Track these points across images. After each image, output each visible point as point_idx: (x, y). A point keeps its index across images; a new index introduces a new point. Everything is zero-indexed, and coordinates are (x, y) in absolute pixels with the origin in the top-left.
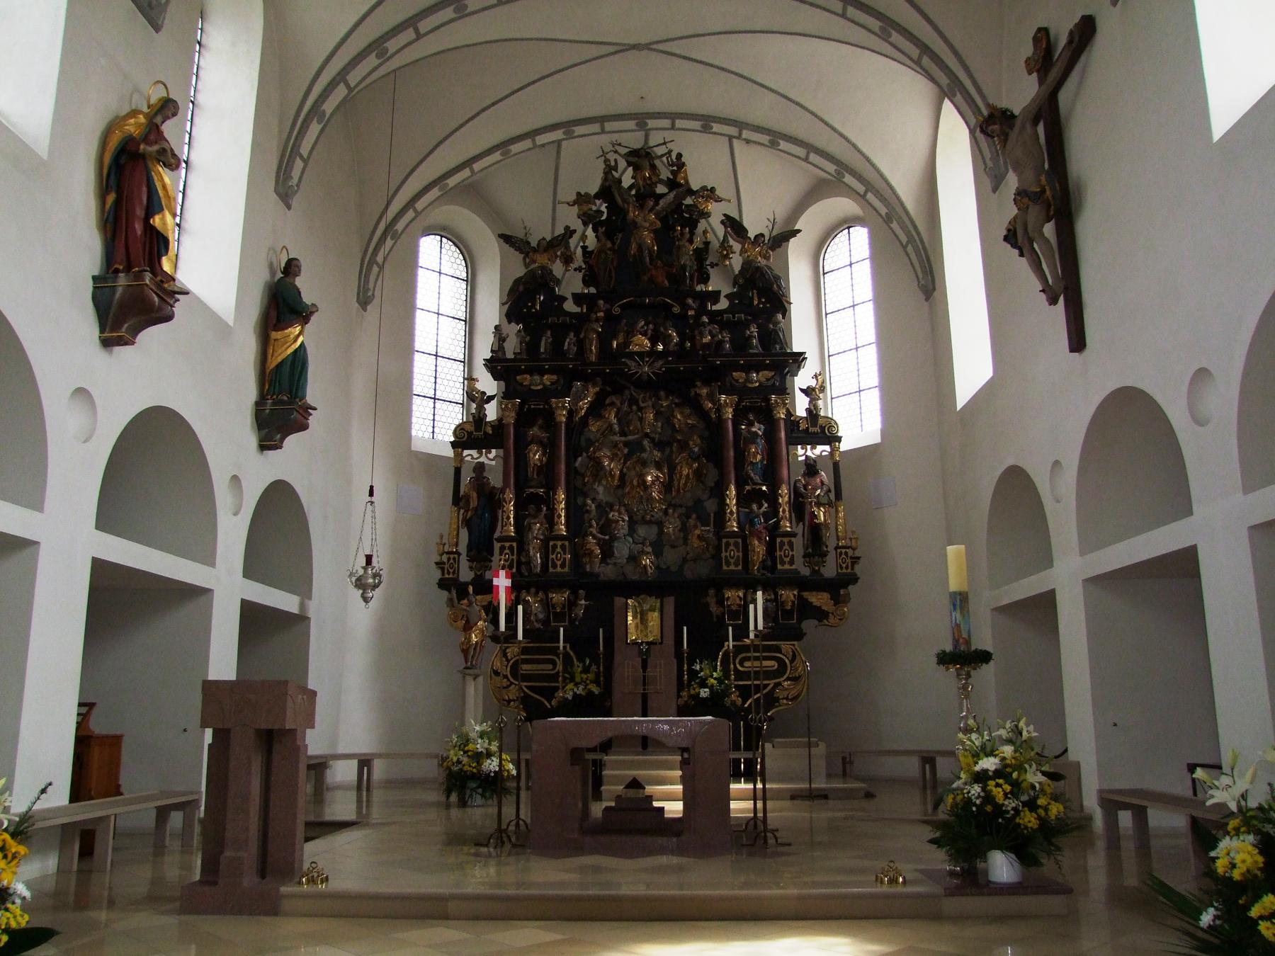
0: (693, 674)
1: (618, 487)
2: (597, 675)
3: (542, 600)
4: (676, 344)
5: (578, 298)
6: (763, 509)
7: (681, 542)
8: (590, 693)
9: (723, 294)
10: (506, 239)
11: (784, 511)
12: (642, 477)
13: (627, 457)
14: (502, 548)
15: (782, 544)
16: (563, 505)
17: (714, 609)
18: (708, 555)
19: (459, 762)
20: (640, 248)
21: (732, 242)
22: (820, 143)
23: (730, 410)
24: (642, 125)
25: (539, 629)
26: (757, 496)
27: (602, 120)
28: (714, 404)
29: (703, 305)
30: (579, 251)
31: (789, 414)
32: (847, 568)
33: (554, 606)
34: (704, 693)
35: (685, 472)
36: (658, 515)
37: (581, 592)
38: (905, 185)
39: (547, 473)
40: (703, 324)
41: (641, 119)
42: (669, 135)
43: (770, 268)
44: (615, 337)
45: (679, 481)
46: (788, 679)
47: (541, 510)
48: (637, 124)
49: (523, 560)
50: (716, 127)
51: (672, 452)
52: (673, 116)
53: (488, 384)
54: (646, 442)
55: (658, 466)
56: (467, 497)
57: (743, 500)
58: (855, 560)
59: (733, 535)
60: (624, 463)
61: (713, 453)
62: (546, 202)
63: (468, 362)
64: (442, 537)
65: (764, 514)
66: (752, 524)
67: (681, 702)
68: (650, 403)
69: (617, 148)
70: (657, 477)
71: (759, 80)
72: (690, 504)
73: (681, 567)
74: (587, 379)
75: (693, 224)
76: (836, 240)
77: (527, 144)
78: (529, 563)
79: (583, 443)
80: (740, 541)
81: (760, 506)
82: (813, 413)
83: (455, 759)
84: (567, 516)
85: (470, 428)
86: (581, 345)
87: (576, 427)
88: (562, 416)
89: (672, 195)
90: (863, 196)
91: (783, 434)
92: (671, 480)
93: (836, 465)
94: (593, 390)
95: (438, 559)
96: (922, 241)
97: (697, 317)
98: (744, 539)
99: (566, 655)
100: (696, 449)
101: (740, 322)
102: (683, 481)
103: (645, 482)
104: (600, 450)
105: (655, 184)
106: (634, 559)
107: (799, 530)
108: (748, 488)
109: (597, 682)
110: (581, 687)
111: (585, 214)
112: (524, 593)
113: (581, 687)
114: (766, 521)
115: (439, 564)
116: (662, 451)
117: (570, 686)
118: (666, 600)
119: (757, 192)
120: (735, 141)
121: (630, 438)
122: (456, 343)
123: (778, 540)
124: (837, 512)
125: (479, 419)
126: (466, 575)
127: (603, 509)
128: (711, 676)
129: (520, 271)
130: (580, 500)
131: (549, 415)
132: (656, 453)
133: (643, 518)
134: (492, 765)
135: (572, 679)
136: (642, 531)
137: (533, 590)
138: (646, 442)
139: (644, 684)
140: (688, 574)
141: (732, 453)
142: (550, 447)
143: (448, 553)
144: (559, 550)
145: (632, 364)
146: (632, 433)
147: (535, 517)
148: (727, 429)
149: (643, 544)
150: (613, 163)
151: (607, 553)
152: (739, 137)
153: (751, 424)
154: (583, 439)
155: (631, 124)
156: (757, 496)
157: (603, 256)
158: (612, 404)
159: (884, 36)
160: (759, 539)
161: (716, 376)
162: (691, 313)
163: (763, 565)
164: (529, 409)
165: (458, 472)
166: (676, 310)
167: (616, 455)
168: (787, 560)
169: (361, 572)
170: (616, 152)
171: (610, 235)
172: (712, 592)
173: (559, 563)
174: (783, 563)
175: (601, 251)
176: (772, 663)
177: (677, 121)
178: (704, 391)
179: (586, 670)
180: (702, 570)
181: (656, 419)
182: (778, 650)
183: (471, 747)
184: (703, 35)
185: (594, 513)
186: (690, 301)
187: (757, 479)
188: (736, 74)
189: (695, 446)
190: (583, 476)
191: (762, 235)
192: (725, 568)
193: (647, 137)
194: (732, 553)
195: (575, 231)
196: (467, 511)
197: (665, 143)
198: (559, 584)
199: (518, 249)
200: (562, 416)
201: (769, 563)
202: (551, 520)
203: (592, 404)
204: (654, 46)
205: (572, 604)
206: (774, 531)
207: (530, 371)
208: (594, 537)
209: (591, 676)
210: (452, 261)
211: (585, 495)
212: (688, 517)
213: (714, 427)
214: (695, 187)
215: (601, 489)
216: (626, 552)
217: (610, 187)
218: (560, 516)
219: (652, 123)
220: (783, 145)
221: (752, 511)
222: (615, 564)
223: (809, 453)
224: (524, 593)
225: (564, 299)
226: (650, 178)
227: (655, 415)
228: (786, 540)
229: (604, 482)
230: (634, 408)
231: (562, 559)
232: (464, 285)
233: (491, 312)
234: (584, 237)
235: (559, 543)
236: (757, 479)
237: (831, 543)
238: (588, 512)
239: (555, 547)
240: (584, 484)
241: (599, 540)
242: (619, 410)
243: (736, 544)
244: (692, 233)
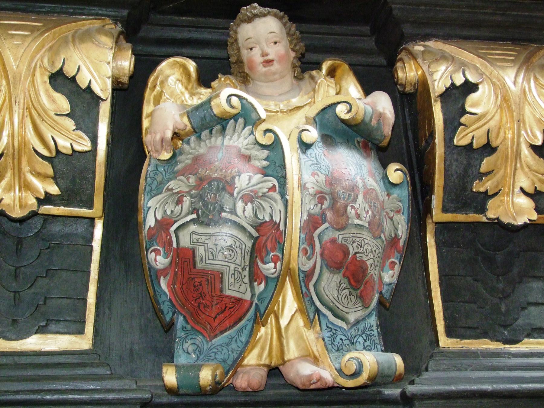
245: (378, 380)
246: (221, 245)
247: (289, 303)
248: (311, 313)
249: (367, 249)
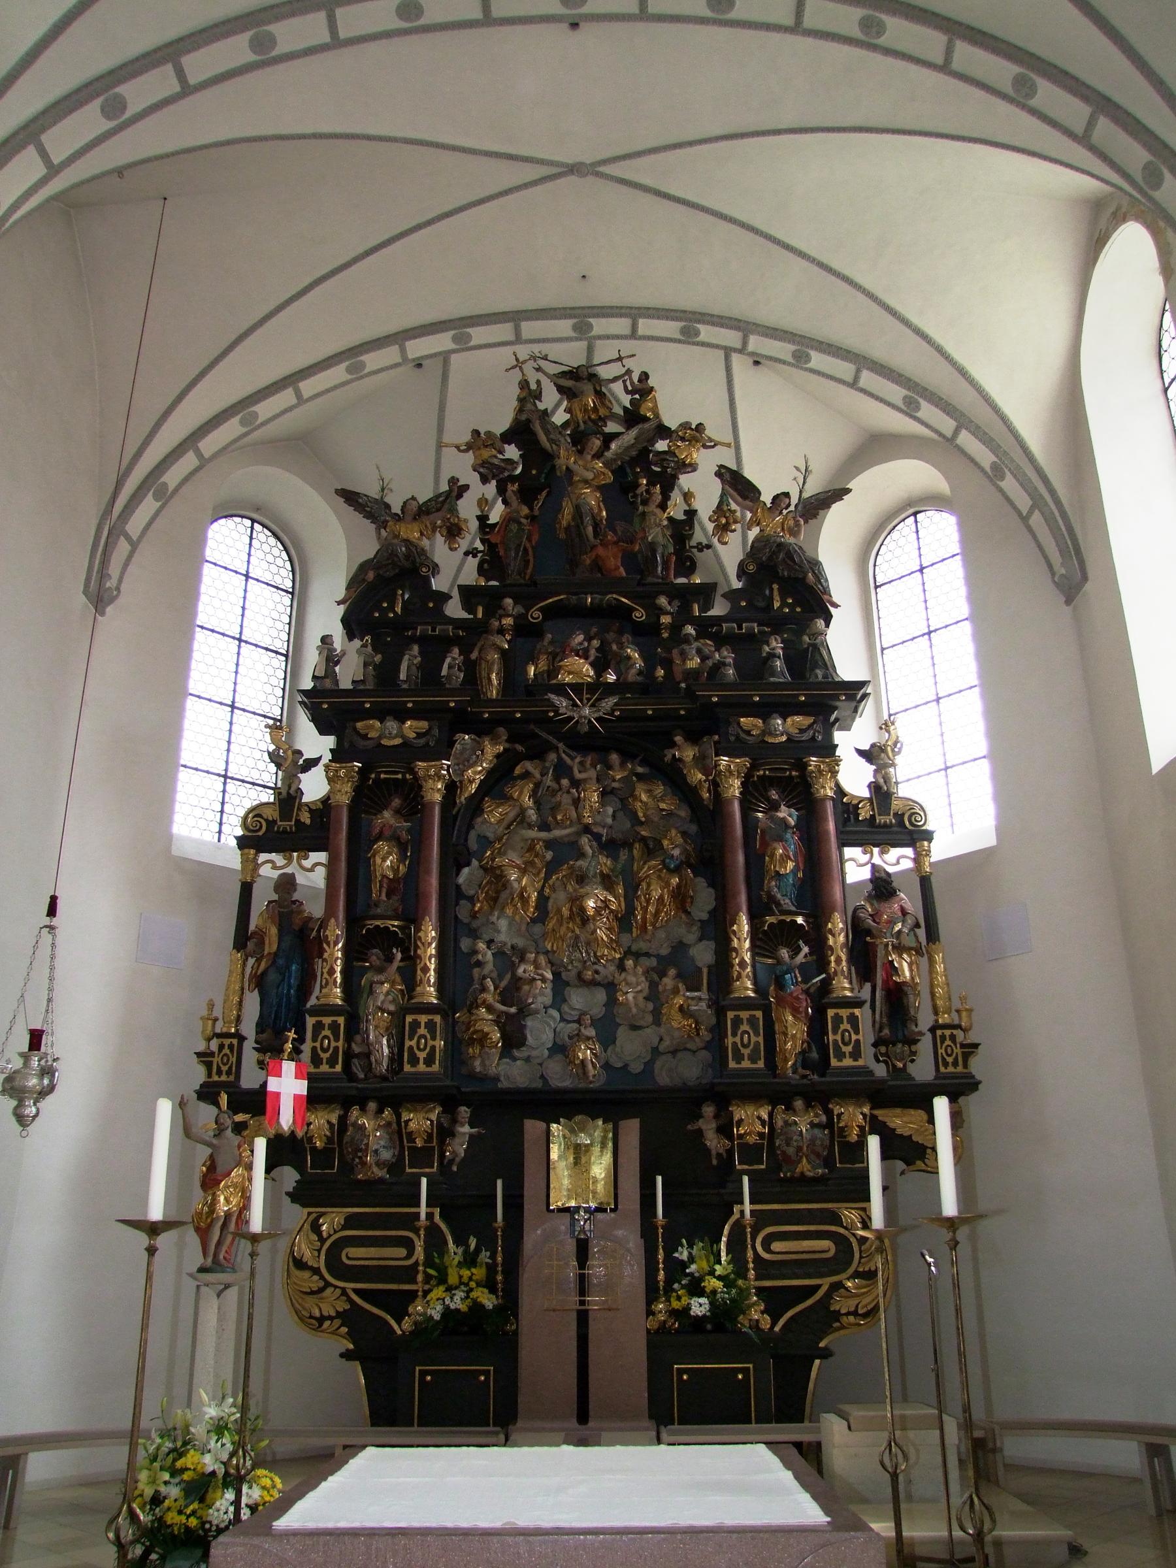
0: (677, 1268)
1: (534, 921)
2: (491, 1269)
3: (389, 1124)
4: (640, 673)
5: (469, 595)
6: (800, 958)
7: (650, 1018)
8: (476, 1307)
9: (721, 591)
10: (350, 497)
11: (838, 961)
12: (577, 903)
13: (552, 868)
14: (318, 1027)
15: (838, 1019)
16: (432, 950)
17: (714, 1142)
18: (698, 1042)
19: (157, 1500)
20: (577, 508)
21: (734, 506)
22: (878, 352)
23: (737, 783)
24: (582, 329)
25: (381, 1180)
26: (788, 934)
27: (516, 317)
28: (706, 772)
29: (685, 608)
30: (474, 525)
31: (840, 792)
32: (955, 1064)
33: (411, 1136)
34: (699, 1307)
35: (656, 893)
36: (608, 971)
37: (463, 1109)
38: (1027, 411)
39: (406, 891)
40: (686, 640)
41: (582, 318)
42: (627, 347)
43: (800, 548)
44: (533, 660)
45: (645, 910)
46: (856, 1275)
47: (390, 959)
48: (575, 328)
49: (356, 1049)
50: (706, 332)
51: (632, 858)
52: (635, 313)
54: (585, 841)
55: (607, 882)
56: (260, 935)
57: (763, 942)
58: (971, 1049)
59: (746, 1004)
60: (546, 879)
61: (708, 861)
62: (425, 443)
64: (211, 1006)
65: (802, 967)
66: (780, 985)
67: (652, 1323)
68: (592, 774)
69: (542, 363)
70: (606, 902)
71: (780, 235)
72: (665, 951)
73: (649, 1065)
74: (482, 729)
75: (668, 483)
76: (895, 534)
77: (391, 354)
79: (473, 844)
80: (759, 1014)
81: (798, 950)
82: (881, 792)
83: (149, 1492)
84: (440, 971)
85: (272, 814)
86: (471, 669)
87: (460, 814)
88: (435, 792)
89: (634, 432)
90: (951, 440)
91: (831, 826)
92: (630, 910)
93: (925, 882)
94: (491, 750)
95: (201, 1047)
96: (1058, 502)
97: (676, 628)
98: (767, 1010)
99: (433, 1232)
100: (676, 852)
101: (750, 636)
102: (651, 909)
103: (583, 910)
104: (501, 853)
105: (604, 420)
106: (560, 1049)
107: (866, 993)
108: (770, 919)
110: (459, 1294)
111: (484, 464)
112: (355, 1112)
113: (459, 1294)
114: (806, 980)
115: (204, 1057)
116: (615, 859)
117: (439, 1292)
118: (623, 1124)
119: (774, 437)
120: (735, 357)
121: (557, 833)
122: (269, 689)
123: (831, 1013)
124: (932, 962)
125: (288, 798)
127: (508, 959)
128: (712, 1273)
129: (369, 549)
130: (465, 944)
132: (603, 859)
133: (579, 975)
135: (442, 1280)
136: (578, 999)
137: (372, 1106)
138: (585, 841)
139: (582, 1292)
140: (664, 1076)
141: (741, 858)
142: (411, 847)
143: (219, 1036)
144: (422, 1031)
145: (562, 703)
146: (559, 825)
147: (380, 970)
148: (731, 815)
149: (578, 1021)
150: (533, 386)
151: (513, 1039)
152: (742, 351)
153: (775, 807)
154: (472, 836)
155: (564, 327)
156: (788, 934)
157: (514, 527)
158: (526, 775)
159: (1019, 96)
160: (795, 1012)
161: (709, 723)
162: (665, 620)
163: (804, 1060)
164: (377, 780)
165: (246, 890)
166: (640, 615)
167: (532, 863)
168: (847, 1049)
169: (18, 1063)
170: (539, 369)
171: (527, 494)
172: (709, 1110)
173: (422, 1055)
174: (840, 1056)
175: (508, 520)
176: (825, 1244)
177: (641, 321)
178: (688, 753)
179: (470, 1260)
180: (690, 1070)
181: (603, 803)
182: (836, 1219)
183: (191, 1459)
184: (691, 144)
185: (489, 967)
186: (663, 601)
187: (787, 903)
188: (743, 225)
189: (674, 846)
190: (472, 900)
191: (787, 495)
192: (732, 1064)
193: (590, 350)
194: (745, 1038)
195: (466, 488)
196: (259, 961)
197: (620, 359)
198: (419, 1094)
199: (370, 516)
200: (435, 792)
201: (815, 1055)
202: (410, 977)
203: (490, 773)
204: (601, 169)
205: (445, 1133)
206: (822, 997)
207: (381, 713)
208: (490, 1009)
209: (479, 1273)
210: (270, 561)
211: (474, 934)
212: (662, 974)
213: (707, 816)
214: (671, 422)
215: (503, 924)
216: (547, 1038)
217: (528, 421)
218: (426, 970)
219: (600, 326)
220: (817, 360)
221: (779, 961)
222: (528, 1059)
223: (877, 860)
224: (355, 1112)
225: (445, 597)
226: (595, 409)
227: (603, 794)
228: (844, 1013)
229: (509, 911)
230: (565, 782)
231: (428, 1049)
232: (287, 600)
233: (326, 619)
235: (423, 1019)
236: (787, 903)
237: (925, 1020)
238: (479, 964)
239: (415, 1025)
240: (474, 916)
241: (500, 1014)
242: (537, 785)
243: (752, 1021)
244: (666, 497)
245: (823, 1175)
246: (791, 1151)
247: (804, 1160)
248: (809, 1163)
249: (819, 1149)
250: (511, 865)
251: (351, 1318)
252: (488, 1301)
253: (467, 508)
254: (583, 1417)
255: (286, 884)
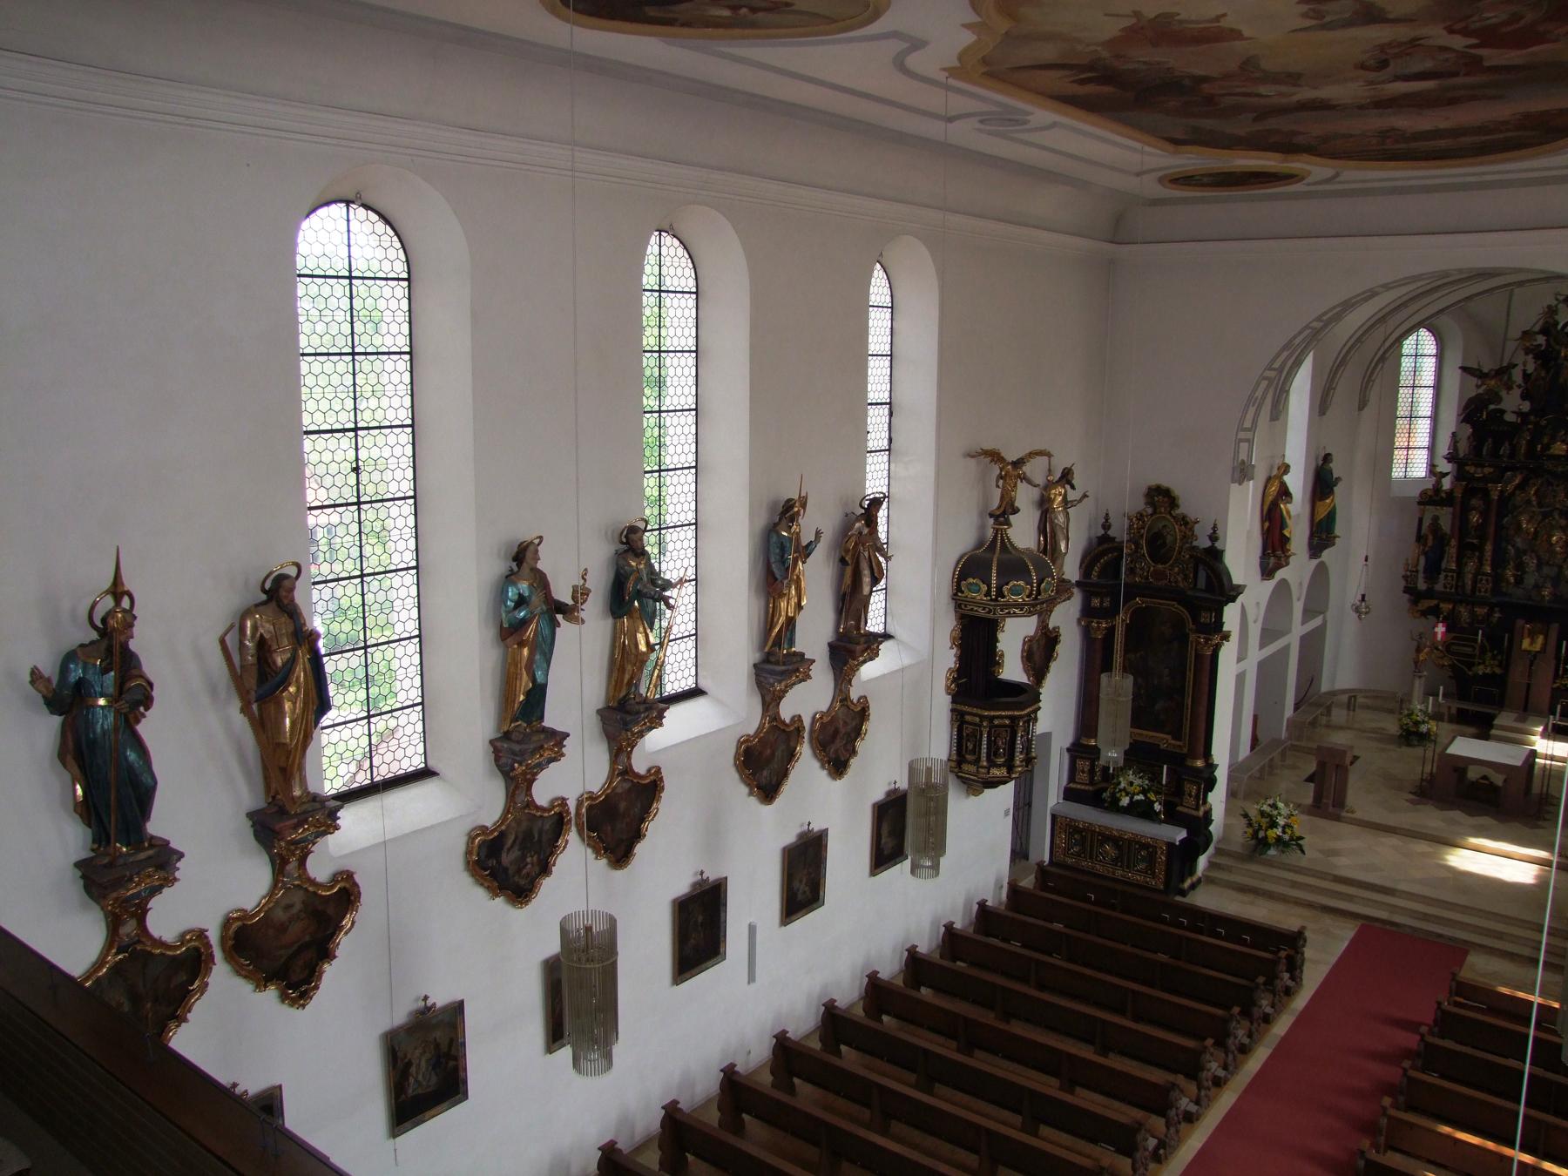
53: (1444, 466)
63: (1432, 449)
74: (1513, 469)
78: (1463, 586)
87: (1504, 499)
88: (1495, 496)
106: (1538, 587)
109: (1500, 666)
125: (1437, 488)
126: (1422, 585)
127: (1520, 553)
131: (1486, 493)
134: (1423, 728)
136: (1546, 570)
142: (1484, 515)
151: (1519, 581)
179: (1494, 658)
200: (1495, 496)
205: (1489, 614)
207: (1476, 466)
231: (1485, 586)
234: (1524, 364)
250: (1523, 518)
251: (1452, 666)
252: (1498, 671)
253: (1517, 376)
254: (1525, 709)
255: (1436, 519)
